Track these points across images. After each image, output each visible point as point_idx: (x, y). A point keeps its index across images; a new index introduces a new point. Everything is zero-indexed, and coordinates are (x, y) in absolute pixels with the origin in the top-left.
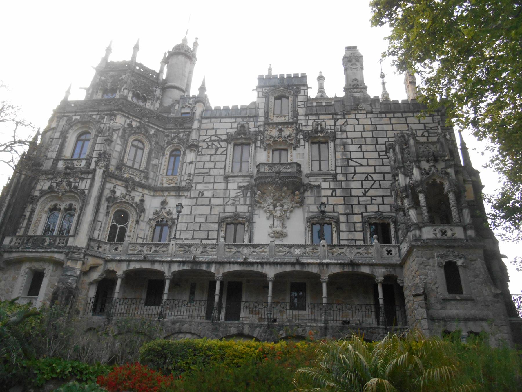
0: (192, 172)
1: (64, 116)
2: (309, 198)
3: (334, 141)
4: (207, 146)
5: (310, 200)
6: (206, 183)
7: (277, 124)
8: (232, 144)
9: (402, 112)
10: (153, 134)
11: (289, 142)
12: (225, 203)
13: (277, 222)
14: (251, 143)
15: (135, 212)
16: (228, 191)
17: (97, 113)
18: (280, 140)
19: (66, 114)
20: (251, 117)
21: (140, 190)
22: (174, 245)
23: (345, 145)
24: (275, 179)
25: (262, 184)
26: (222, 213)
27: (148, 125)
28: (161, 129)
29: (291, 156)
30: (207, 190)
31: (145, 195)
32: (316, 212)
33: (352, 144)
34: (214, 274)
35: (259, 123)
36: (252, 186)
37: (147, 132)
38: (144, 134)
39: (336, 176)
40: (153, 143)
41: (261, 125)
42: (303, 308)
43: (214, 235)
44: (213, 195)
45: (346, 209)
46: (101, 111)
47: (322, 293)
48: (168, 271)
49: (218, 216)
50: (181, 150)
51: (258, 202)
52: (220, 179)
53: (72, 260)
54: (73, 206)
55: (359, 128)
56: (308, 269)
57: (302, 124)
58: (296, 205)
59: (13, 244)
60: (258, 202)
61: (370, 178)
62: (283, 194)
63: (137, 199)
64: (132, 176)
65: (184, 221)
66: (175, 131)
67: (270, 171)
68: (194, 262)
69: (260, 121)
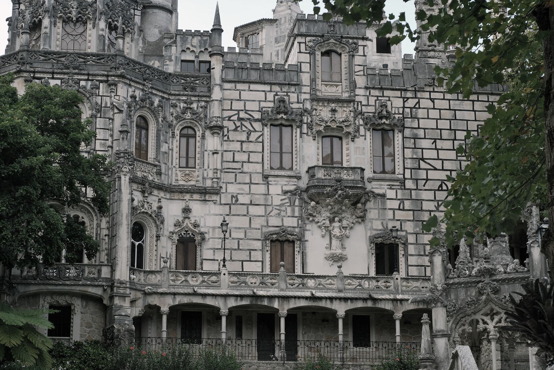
0: (219, 167)
1: (34, 78)
2: (372, 211)
3: (402, 131)
4: (234, 127)
5: (372, 214)
6: (240, 183)
7: (330, 101)
8: (269, 126)
9: (488, 94)
10: (159, 106)
11: (346, 130)
12: (268, 213)
13: (335, 242)
14: (294, 127)
15: (154, 225)
16: (270, 197)
17: (86, 77)
18: (334, 125)
19: (38, 75)
20: (292, 85)
21: (156, 192)
22: (227, 274)
23: (415, 138)
24: (336, 190)
25: (319, 194)
26: (265, 226)
27: (152, 93)
28: (166, 96)
29: (348, 149)
30: (242, 194)
31: (162, 200)
32: (380, 230)
33: (425, 138)
34: (278, 310)
35: (304, 96)
36: (301, 191)
37: (152, 104)
38: (149, 108)
39: (404, 183)
40: (160, 120)
41: (307, 100)
42: (367, 344)
43: (257, 255)
44: (251, 201)
45: (416, 226)
46: (93, 75)
47: (395, 332)
48: (224, 306)
49: (260, 231)
50: (196, 129)
51: (311, 215)
52: (258, 178)
53: (119, 296)
54: (80, 220)
55: (434, 114)
56: (381, 305)
57: (361, 102)
58: (357, 220)
59: (25, 273)
60: (311, 215)
61: (444, 187)
62: (344, 208)
63: (155, 206)
64: (145, 174)
65: (217, 236)
66: (184, 98)
67: (327, 177)
68: (255, 296)
69: (305, 93)
